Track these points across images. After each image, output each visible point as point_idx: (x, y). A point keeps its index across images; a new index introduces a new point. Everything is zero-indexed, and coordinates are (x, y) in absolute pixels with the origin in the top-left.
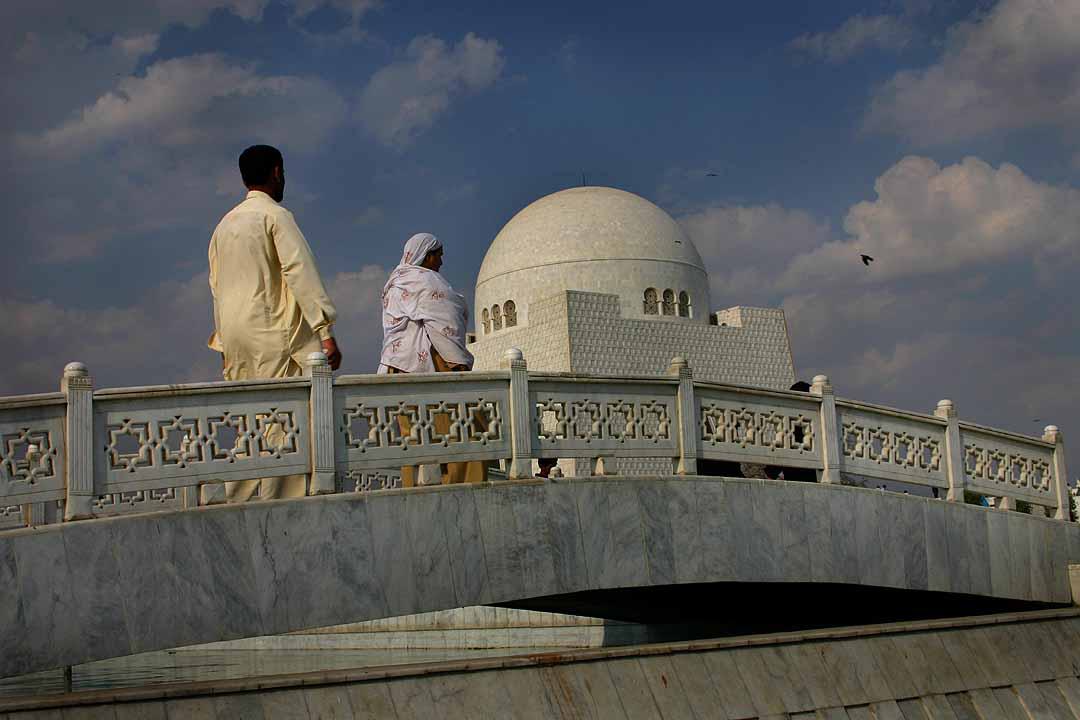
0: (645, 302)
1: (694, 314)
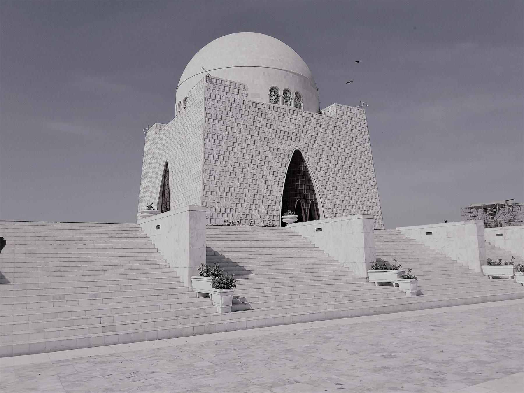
0: (271, 96)
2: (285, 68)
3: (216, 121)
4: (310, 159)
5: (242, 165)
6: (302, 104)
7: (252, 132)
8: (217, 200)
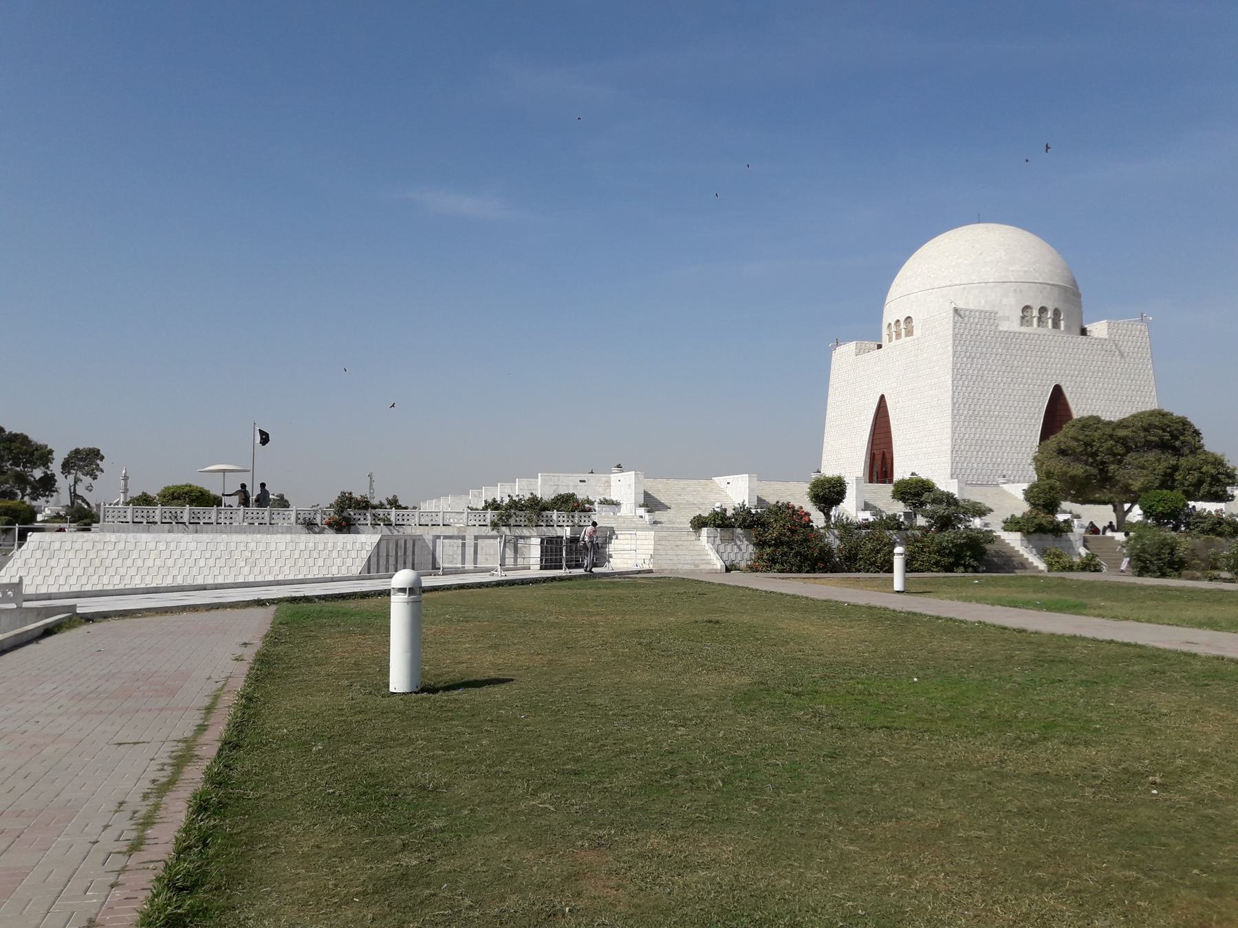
0: (1023, 318)
6: (1062, 323)
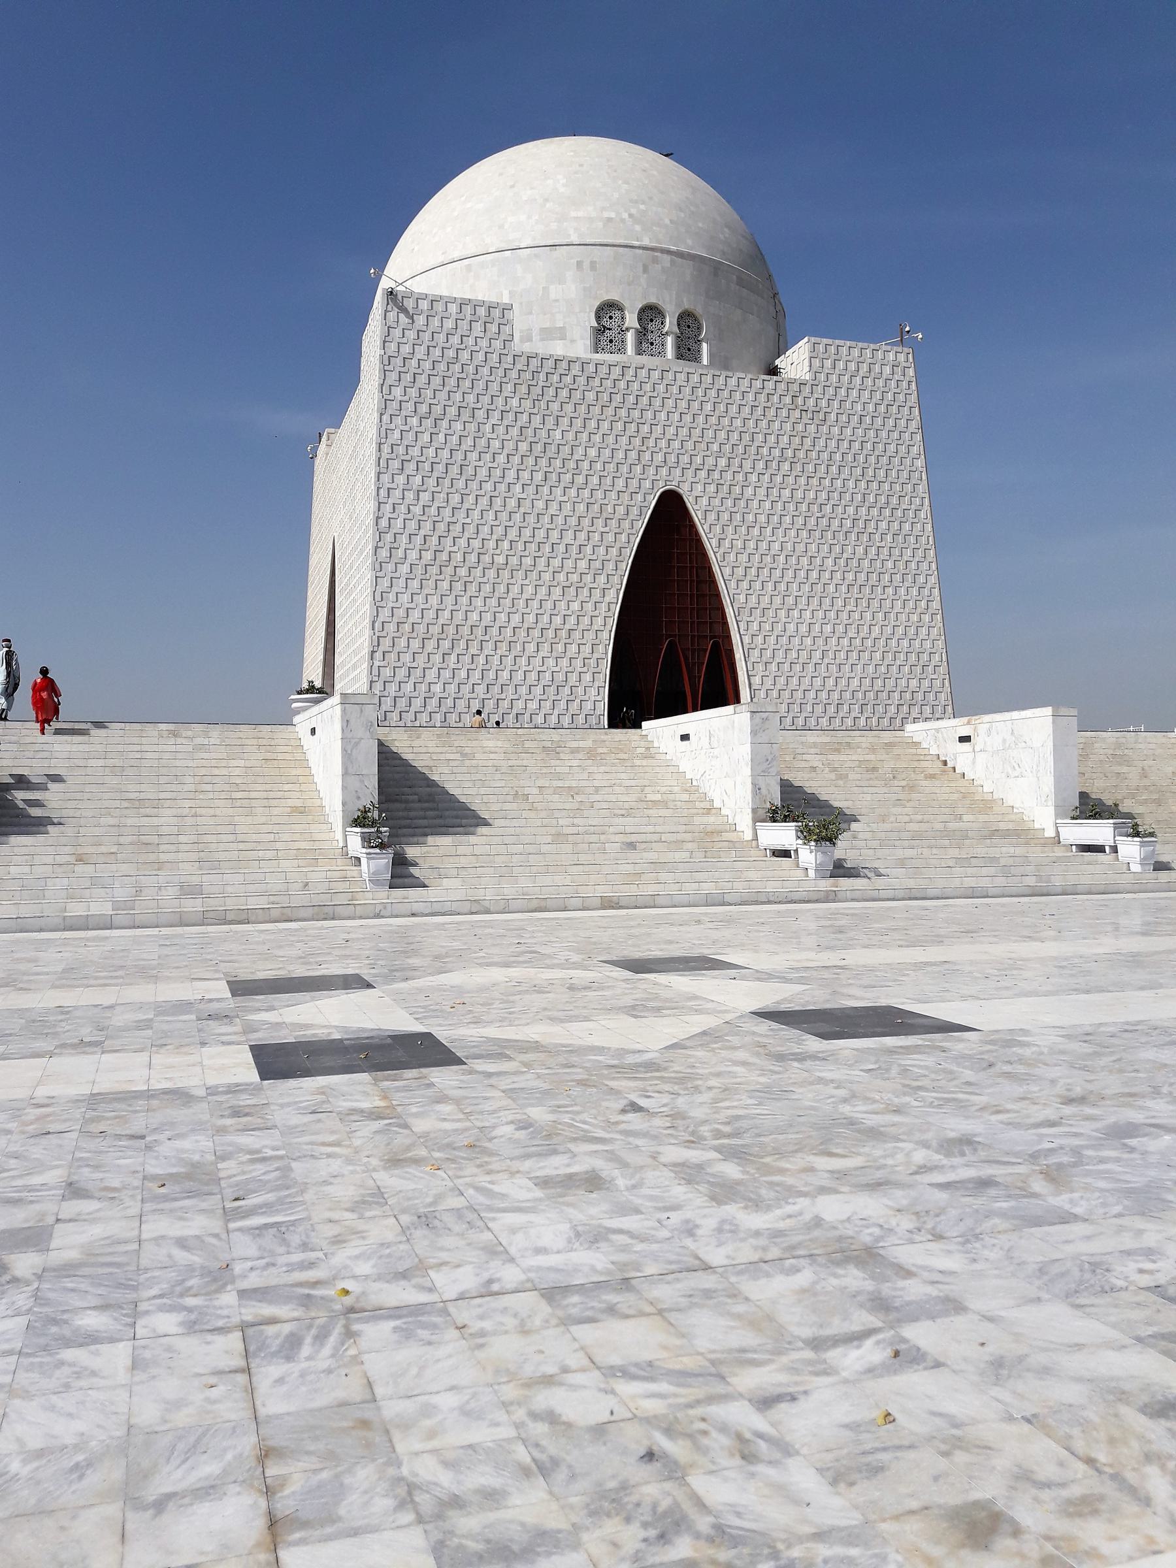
0: (600, 331)
1: (711, 355)
2: (646, 242)
3: (415, 421)
4: (712, 517)
5: (491, 544)
6: (705, 346)
7: (524, 447)
8: (415, 645)
